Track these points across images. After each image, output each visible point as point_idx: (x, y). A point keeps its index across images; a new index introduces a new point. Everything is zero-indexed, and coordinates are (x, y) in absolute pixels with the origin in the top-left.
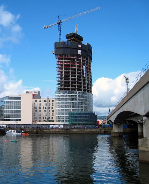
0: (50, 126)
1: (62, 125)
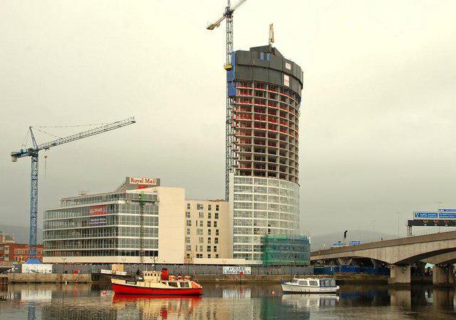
0: (224, 267)
1: (249, 265)
